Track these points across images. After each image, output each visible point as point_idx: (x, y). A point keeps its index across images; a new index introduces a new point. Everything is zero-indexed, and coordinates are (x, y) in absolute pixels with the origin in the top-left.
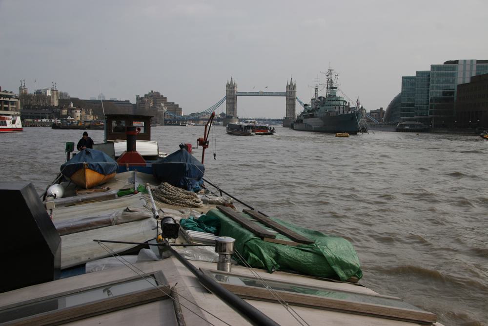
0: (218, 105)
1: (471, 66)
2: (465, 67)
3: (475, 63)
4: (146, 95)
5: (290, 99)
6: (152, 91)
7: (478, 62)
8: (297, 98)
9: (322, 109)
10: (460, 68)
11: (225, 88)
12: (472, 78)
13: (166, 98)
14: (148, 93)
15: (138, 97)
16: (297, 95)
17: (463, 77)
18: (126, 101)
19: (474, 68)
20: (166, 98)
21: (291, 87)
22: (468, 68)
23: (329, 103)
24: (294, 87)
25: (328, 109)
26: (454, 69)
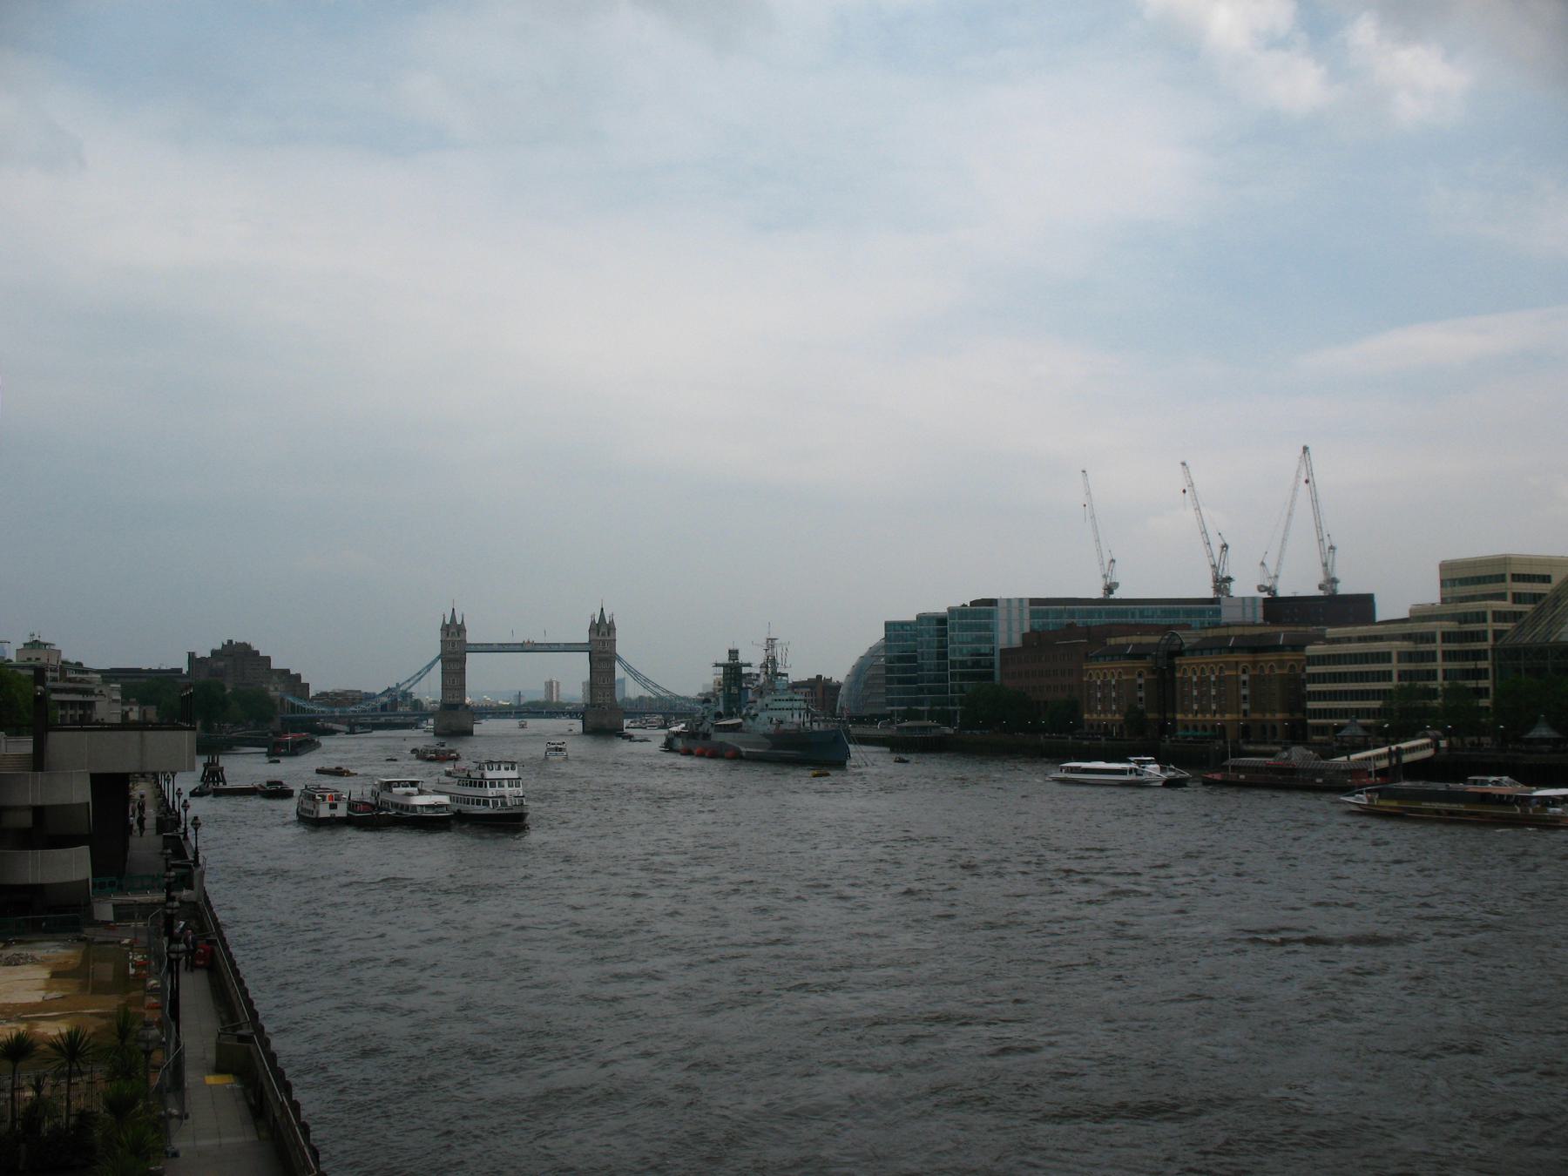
0: (420, 675)
1: (1021, 611)
2: (1009, 612)
3: (1026, 604)
4: (214, 652)
5: (600, 660)
6: (230, 642)
7: (1033, 602)
8: (620, 659)
9: (763, 716)
10: (1001, 613)
11: (437, 636)
12: (1025, 636)
13: (268, 659)
14: (219, 647)
15: (191, 656)
16: (620, 649)
17: (1008, 634)
18: (173, 670)
19: (1027, 615)
20: (268, 659)
21: (603, 629)
22: (1015, 614)
23: (777, 705)
24: (611, 628)
25: (776, 715)
26: (990, 615)
